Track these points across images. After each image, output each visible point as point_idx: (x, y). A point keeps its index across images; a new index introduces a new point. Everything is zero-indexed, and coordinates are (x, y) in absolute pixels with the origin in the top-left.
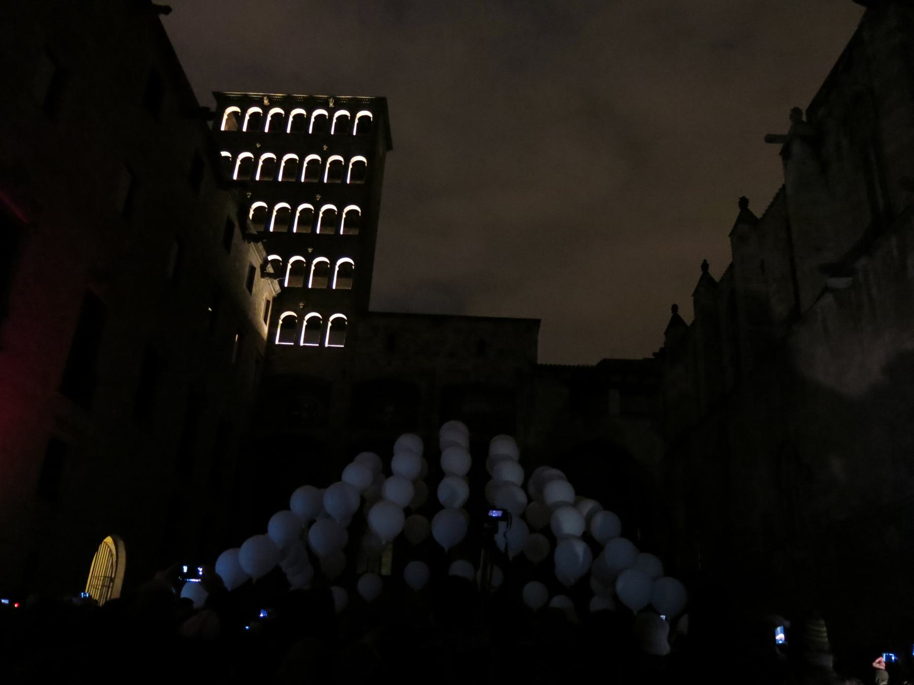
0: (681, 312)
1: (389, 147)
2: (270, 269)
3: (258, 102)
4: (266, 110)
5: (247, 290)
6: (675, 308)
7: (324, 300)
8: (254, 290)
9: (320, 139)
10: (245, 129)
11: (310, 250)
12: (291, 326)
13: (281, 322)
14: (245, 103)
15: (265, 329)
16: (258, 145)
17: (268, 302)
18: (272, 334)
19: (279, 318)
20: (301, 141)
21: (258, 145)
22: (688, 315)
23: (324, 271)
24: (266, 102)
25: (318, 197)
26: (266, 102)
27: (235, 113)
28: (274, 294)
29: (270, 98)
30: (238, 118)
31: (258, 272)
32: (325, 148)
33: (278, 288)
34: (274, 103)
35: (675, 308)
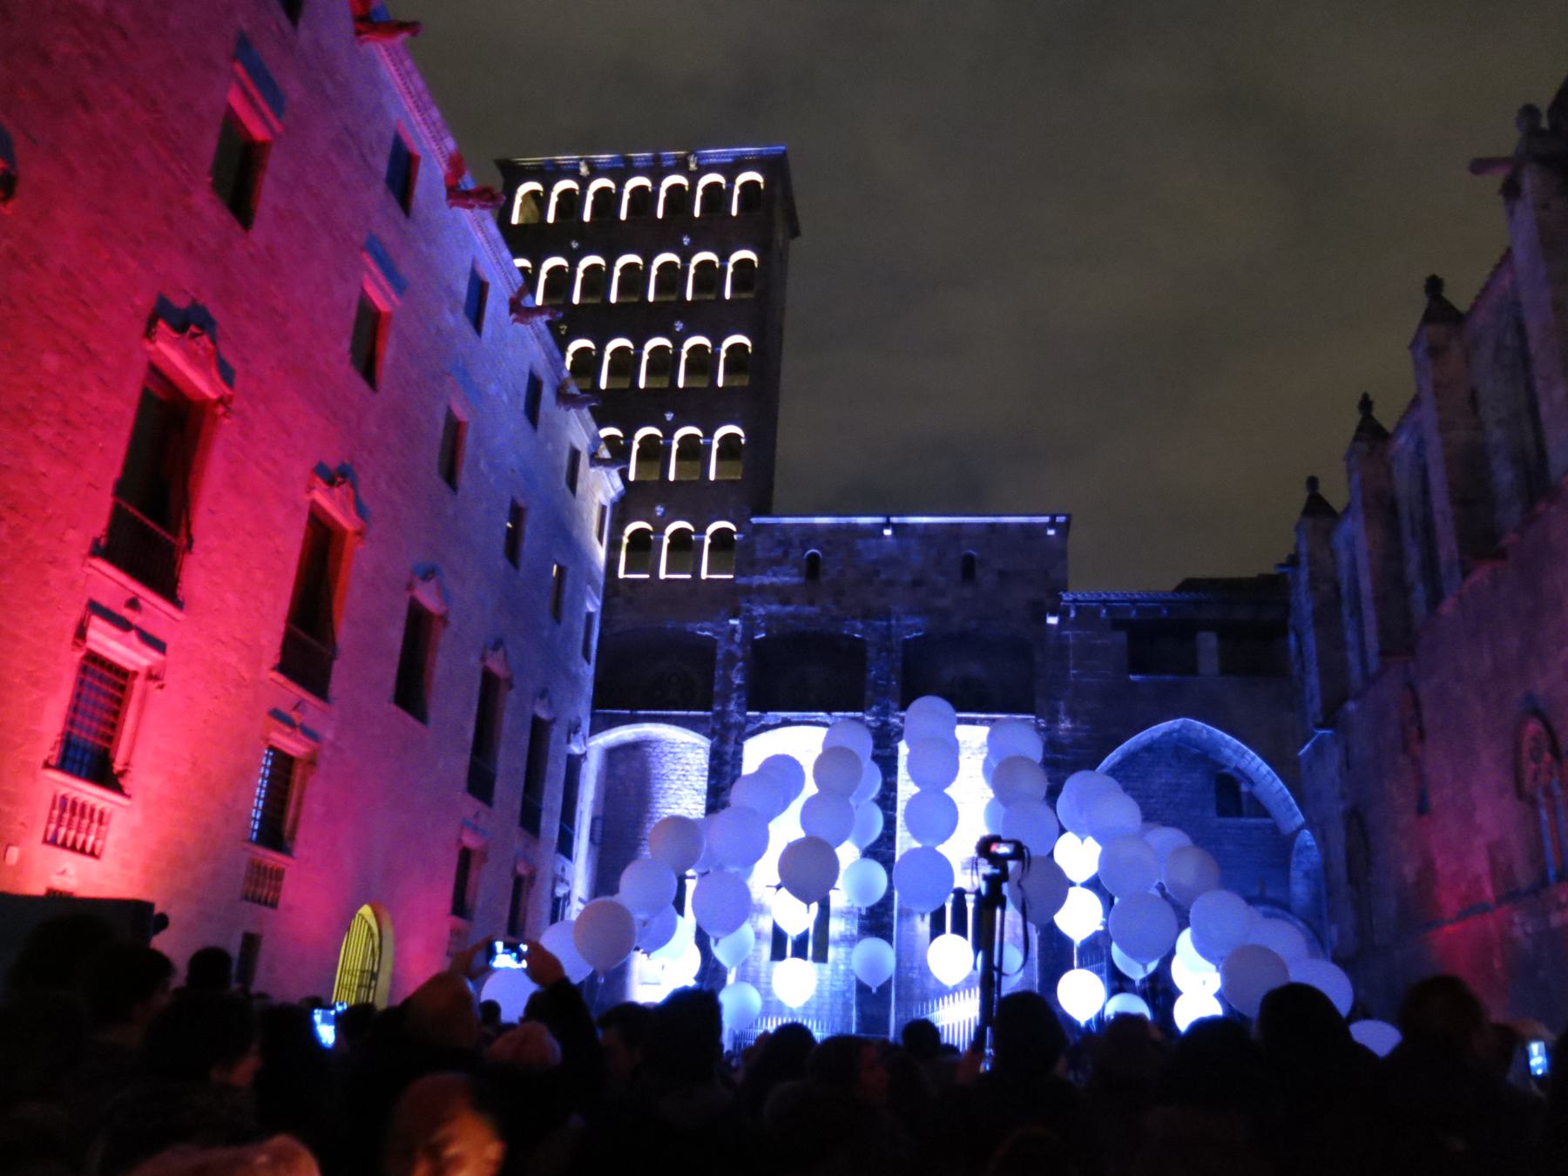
0: (1323, 489)
1: (795, 232)
2: (605, 454)
3: (573, 173)
4: (584, 183)
5: (568, 491)
6: (1312, 482)
7: (696, 499)
8: (580, 487)
9: (677, 225)
10: (551, 218)
11: (669, 416)
12: (642, 546)
14: (549, 175)
15: (601, 553)
16: (575, 245)
17: (603, 508)
18: (612, 564)
19: (622, 533)
20: (645, 230)
21: (575, 245)
22: (1337, 494)
23: (692, 450)
24: (584, 170)
25: (679, 326)
26: (584, 170)
27: (534, 193)
28: (613, 494)
29: (591, 165)
31: (584, 459)
32: (686, 240)
33: (618, 484)
34: (595, 172)
35: (1312, 482)
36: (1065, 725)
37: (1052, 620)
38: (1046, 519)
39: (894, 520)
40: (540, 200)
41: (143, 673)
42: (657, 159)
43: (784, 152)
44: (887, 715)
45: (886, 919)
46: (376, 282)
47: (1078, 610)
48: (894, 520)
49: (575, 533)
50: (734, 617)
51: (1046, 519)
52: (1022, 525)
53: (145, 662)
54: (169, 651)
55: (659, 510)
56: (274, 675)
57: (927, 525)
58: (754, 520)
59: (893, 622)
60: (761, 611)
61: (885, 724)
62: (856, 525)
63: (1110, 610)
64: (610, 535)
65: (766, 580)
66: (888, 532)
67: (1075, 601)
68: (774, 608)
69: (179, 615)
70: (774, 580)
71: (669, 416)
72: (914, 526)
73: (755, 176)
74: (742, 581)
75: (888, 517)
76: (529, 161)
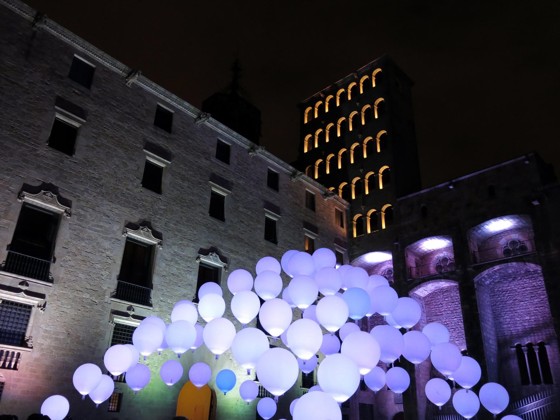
7: (377, 198)
8: (317, 208)
9: (358, 100)
13: (355, 223)
15: (344, 231)
29: (323, 93)
32: (358, 104)
37: (536, 203)
38: (524, 157)
39: (454, 181)
40: (312, 113)
41: (36, 305)
46: (150, 156)
48: (454, 181)
50: (397, 241)
51: (524, 157)
53: (37, 302)
54: (47, 296)
56: (113, 299)
57: (469, 178)
58: (398, 200)
64: (347, 222)
66: (451, 187)
69: (50, 284)
71: (361, 171)
72: (463, 180)
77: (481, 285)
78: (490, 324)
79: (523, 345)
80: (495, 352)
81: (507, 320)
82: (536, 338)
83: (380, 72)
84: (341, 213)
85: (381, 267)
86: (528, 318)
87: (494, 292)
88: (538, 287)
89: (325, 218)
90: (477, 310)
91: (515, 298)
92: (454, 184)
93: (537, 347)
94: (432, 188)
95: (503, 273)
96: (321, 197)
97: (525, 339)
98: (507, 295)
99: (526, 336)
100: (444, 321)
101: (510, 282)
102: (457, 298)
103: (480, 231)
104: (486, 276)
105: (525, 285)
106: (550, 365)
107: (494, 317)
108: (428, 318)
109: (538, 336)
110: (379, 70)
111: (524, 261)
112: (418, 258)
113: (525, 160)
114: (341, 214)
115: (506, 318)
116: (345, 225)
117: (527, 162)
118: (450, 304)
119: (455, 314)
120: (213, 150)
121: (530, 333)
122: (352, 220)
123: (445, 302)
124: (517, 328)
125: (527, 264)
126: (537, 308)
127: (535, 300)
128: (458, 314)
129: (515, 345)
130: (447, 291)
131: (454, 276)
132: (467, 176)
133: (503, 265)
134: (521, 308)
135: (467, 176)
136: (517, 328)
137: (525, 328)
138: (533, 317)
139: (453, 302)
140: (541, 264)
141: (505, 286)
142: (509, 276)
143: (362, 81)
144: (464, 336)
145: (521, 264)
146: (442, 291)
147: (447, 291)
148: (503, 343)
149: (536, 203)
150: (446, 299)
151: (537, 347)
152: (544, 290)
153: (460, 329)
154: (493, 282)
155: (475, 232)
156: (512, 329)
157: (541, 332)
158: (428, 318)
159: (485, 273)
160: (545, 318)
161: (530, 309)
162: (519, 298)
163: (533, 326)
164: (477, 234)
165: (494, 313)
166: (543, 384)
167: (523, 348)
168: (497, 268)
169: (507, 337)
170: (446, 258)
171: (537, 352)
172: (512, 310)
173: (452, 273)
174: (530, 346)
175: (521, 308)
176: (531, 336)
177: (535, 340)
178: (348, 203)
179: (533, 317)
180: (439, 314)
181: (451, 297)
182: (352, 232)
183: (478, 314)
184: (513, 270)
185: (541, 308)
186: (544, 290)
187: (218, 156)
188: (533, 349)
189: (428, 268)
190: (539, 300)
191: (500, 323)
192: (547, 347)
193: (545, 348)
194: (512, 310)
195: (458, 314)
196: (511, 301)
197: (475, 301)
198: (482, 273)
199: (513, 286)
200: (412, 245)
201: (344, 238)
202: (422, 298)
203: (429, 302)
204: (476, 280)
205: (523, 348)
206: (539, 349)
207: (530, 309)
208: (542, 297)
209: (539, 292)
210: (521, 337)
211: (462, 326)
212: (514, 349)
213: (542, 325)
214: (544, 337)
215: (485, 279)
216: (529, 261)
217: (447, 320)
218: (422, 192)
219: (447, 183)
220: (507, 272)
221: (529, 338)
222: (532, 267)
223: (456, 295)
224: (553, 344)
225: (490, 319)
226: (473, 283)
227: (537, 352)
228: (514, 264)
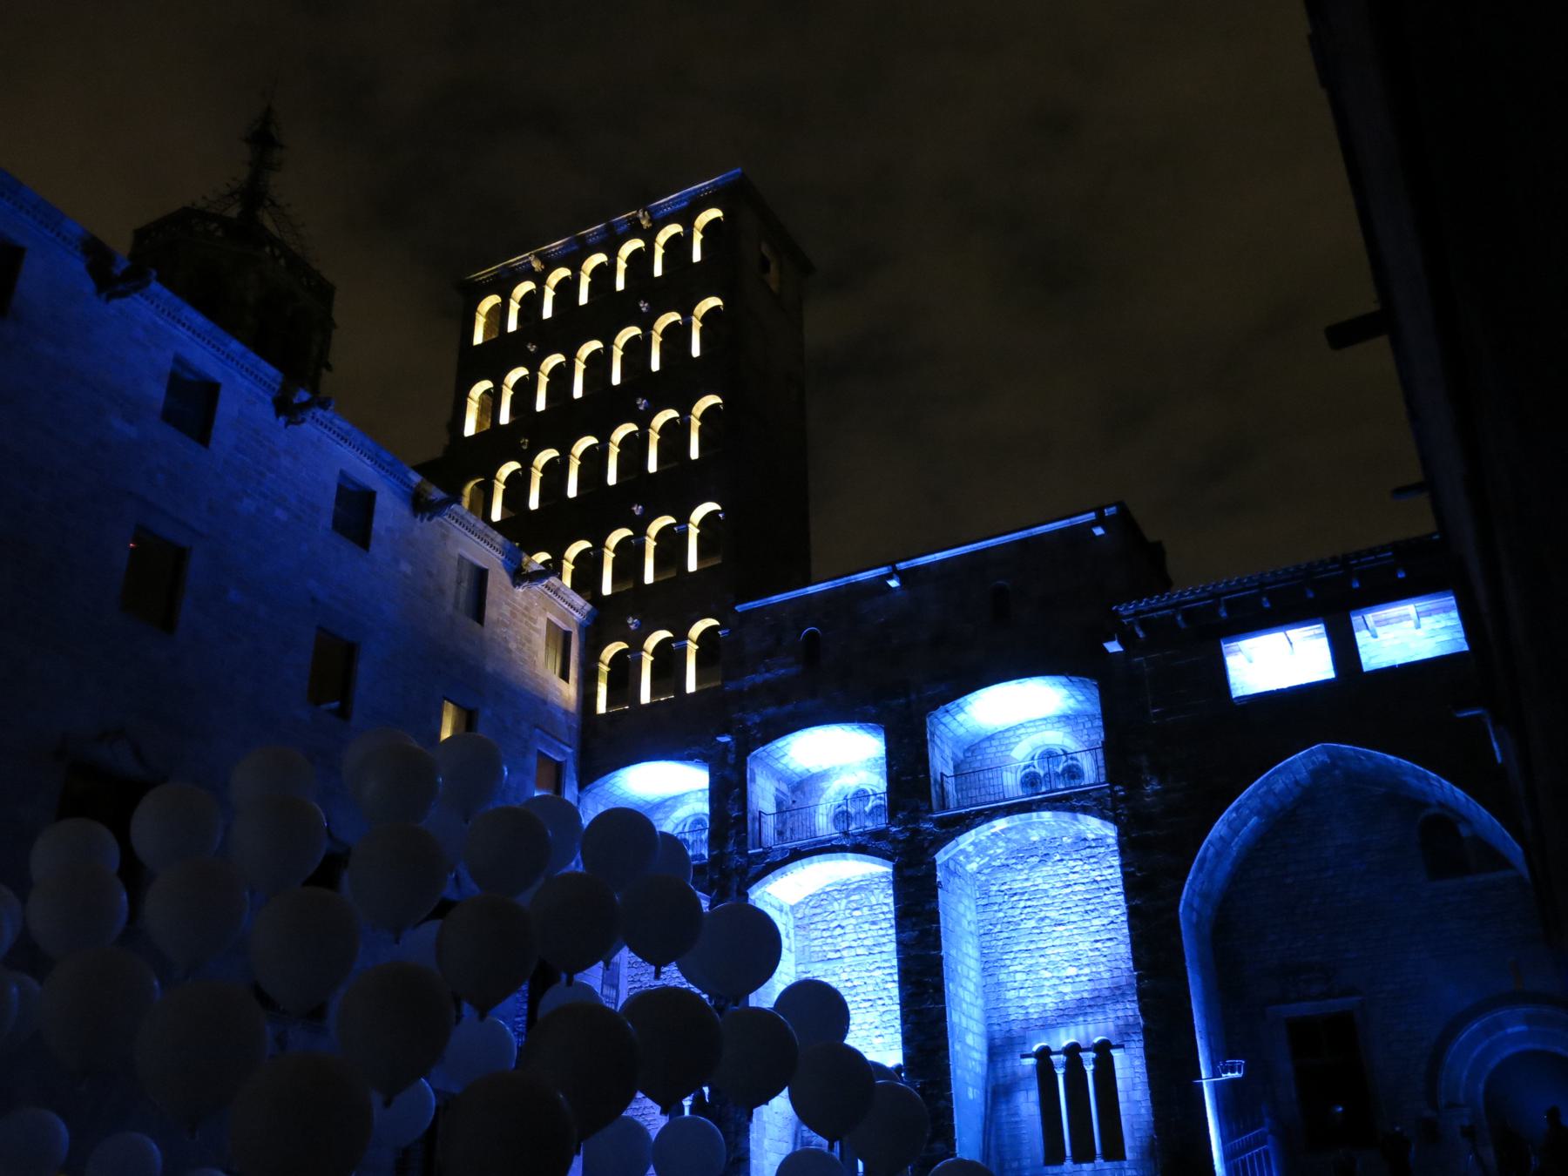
3: (528, 274)
7: (674, 601)
8: (491, 612)
9: (648, 294)
11: (637, 510)
12: (624, 672)
15: (568, 692)
16: (532, 348)
20: (608, 311)
21: (532, 348)
24: (537, 265)
25: (642, 404)
26: (537, 265)
29: (539, 256)
30: (500, 312)
31: (498, 578)
32: (644, 306)
36: (1152, 787)
37: (1113, 647)
38: (1091, 516)
39: (902, 566)
40: (500, 312)
42: (610, 228)
43: (743, 174)
44: (916, 820)
45: (942, 1103)
47: (1144, 624)
48: (902, 566)
49: (490, 667)
51: (1091, 516)
52: (1061, 531)
55: (632, 623)
59: (913, 697)
60: (757, 719)
61: (916, 832)
62: (858, 583)
63: (1189, 615)
65: (759, 679)
66: (893, 583)
67: (1137, 614)
68: (771, 710)
70: (768, 675)
71: (637, 510)
73: (714, 213)
74: (730, 687)
75: (893, 564)
76: (483, 274)
77: (954, 873)
78: (972, 988)
79: (1054, 1049)
80: (978, 1069)
81: (1019, 977)
82: (1091, 1028)
83: (717, 219)
84: (567, 636)
85: (673, 808)
86: (1072, 971)
87: (987, 894)
88: (1104, 885)
89: (513, 645)
90: (939, 947)
91: (1042, 914)
92: (902, 576)
93: (1092, 1055)
94: (840, 582)
95: (1015, 841)
96: (507, 580)
97: (1062, 1031)
98: (1022, 904)
99: (1063, 1025)
100: (844, 976)
101: (1031, 869)
102: (885, 909)
103: (961, 717)
104: (970, 849)
105: (1072, 876)
106: (1122, 1107)
107: (984, 969)
108: (801, 968)
109: (1096, 1022)
110: (714, 213)
111: (1072, 810)
112: (784, 788)
113: (1094, 524)
114: (567, 636)
115: (1016, 973)
116: (573, 673)
117: (1099, 531)
118: (866, 927)
119: (877, 958)
120: (157, 392)
121: (1077, 1015)
122: (596, 658)
123: (853, 921)
124: (1042, 1001)
125: (1080, 816)
126: (1099, 945)
127: (1096, 922)
128: (885, 956)
129: (1035, 1049)
130: (859, 889)
131: (882, 845)
132: (939, 556)
133: (1017, 819)
134: (1057, 942)
135: (939, 556)
136: (1042, 1001)
137: (1064, 1002)
138: (1086, 970)
139: (874, 923)
140: (1115, 820)
141: (1018, 879)
142: (1031, 850)
143: (663, 237)
144: (897, 1023)
145: (1065, 816)
146: (847, 889)
147: (859, 889)
148: (1000, 1047)
149: (1113, 647)
150: (856, 913)
151: (1092, 1055)
152: (1118, 894)
153: (887, 1001)
154: (988, 865)
155: (947, 719)
156: (1027, 1003)
157: (1105, 1012)
158: (801, 968)
159: (967, 840)
160: (1116, 973)
161: (1081, 946)
162: (1053, 914)
163: (1086, 995)
164: (954, 725)
165: (983, 955)
166: (1099, 1161)
167: (1053, 1058)
168: (1000, 824)
169: (1015, 1027)
170: (864, 791)
171: (1089, 1069)
172: (1032, 946)
173: (877, 835)
174: (1073, 1051)
175: (1057, 942)
176: (1077, 1024)
177: (1087, 1034)
178: (588, 607)
179: (1086, 970)
180: (831, 955)
181: (871, 907)
182: (594, 695)
183: (941, 958)
184: (1043, 833)
185: (1109, 944)
186: (1118, 894)
187: (168, 416)
188: (1080, 1061)
189: (811, 817)
190: (1106, 921)
191: (998, 984)
192: (1117, 1054)
193: (1111, 1058)
194: (1032, 946)
195: (885, 956)
196: (1032, 923)
197: (934, 916)
198: (960, 839)
199: (1040, 881)
200: (771, 747)
201: (566, 712)
202: (786, 908)
203: (806, 921)
204: (941, 857)
205: (1053, 1058)
206: (1095, 1061)
207: (1081, 946)
208: (1113, 912)
209: (1105, 899)
210: (1053, 1026)
211: (895, 992)
212: (1031, 1061)
213: (1106, 993)
214: (1111, 1026)
215: (967, 855)
216: (1086, 811)
217: (855, 975)
218: (811, 590)
219: (883, 570)
220: (1027, 839)
221: (1072, 1030)
222: (1093, 826)
223: (884, 900)
224: (1133, 1045)
225: (972, 974)
226: (933, 865)
227: (1089, 1069)
228: (1047, 815)
